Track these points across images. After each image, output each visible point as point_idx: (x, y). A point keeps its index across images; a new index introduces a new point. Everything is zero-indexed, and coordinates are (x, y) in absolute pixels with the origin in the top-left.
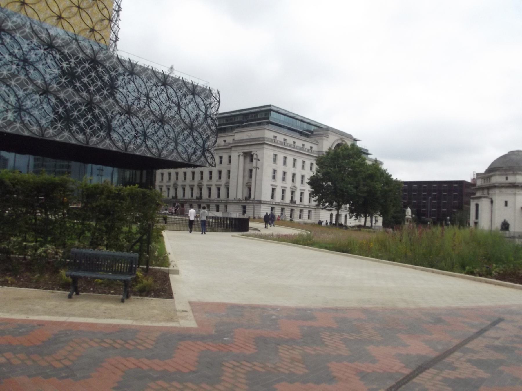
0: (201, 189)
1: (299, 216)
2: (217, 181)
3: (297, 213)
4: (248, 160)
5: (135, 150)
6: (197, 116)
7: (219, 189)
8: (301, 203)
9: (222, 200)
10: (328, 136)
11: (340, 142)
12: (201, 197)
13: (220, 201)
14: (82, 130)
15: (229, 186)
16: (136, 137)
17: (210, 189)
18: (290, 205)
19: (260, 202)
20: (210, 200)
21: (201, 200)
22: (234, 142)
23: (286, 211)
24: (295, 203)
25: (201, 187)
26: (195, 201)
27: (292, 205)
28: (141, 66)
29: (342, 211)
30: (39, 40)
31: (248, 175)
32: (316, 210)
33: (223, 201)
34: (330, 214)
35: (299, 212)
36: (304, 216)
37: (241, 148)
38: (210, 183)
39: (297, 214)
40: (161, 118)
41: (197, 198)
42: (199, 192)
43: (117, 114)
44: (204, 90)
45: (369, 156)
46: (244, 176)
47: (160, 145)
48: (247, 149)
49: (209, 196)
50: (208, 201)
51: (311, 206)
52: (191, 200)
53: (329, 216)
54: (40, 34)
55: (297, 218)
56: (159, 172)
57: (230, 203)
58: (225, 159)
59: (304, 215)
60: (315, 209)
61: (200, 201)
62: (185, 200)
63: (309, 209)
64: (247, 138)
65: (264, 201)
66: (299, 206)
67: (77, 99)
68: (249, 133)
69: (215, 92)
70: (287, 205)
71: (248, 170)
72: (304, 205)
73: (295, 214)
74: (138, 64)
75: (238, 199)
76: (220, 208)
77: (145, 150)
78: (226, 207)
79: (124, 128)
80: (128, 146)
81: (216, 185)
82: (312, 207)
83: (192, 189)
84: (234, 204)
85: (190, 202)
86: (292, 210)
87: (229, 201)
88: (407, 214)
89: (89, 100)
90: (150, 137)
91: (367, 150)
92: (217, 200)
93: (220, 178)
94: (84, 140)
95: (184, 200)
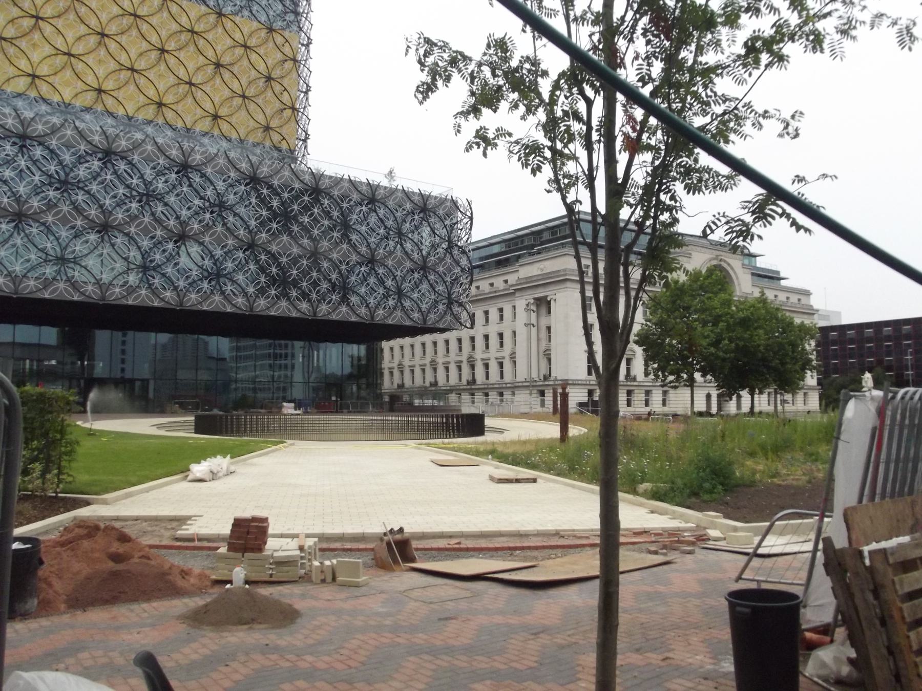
0: (473, 367)
1: (644, 402)
2: (498, 351)
4: (543, 311)
5: (386, 318)
6: (434, 246)
7: (501, 365)
9: (506, 384)
10: (690, 254)
11: (715, 262)
13: (504, 386)
14: (305, 296)
16: (386, 297)
17: (487, 366)
18: (625, 383)
26: (465, 387)
27: (629, 383)
28: (331, 177)
30: (168, 160)
33: (508, 385)
34: (705, 395)
35: (644, 395)
37: (529, 292)
39: (640, 399)
40: (422, 264)
43: (355, 265)
44: (442, 201)
45: (783, 283)
46: (538, 340)
47: (425, 306)
48: (540, 293)
49: (487, 378)
50: (486, 386)
53: (705, 399)
54: (168, 151)
56: (385, 345)
58: (507, 313)
61: (473, 387)
64: (540, 273)
66: (642, 384)
67: (296, 250)
68: (541, 265)
69: (463, 202)
74: (325, 173)
77: (401, 317)
79: (368, 284)
80: (375, 312)
81: (497, 358)
83: (460, 368)
85: (457, 390)
87: (517, 385)
88: (864, 384)
89: (313, 249)
90: (408, 294)
91: (778, 272)
94: (309, 311)
95: (448, 388)
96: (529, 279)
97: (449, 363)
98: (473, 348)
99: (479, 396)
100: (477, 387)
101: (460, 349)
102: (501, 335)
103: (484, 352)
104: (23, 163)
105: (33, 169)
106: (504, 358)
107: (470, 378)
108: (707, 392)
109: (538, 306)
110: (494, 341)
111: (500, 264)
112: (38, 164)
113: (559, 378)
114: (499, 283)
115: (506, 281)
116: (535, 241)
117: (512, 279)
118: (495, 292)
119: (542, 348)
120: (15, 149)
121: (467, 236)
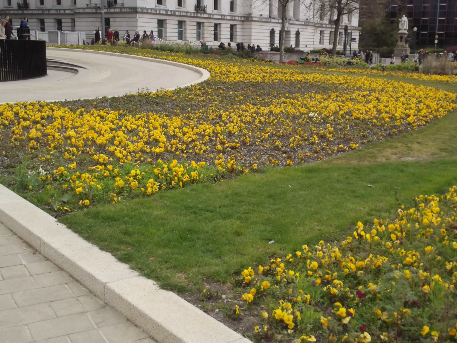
1: (213, 36)
3: (209, 31)
8: (215, 12)
9: (65, 10)
13: (62, 12)
19: (134, 11)
21: (26, 10)
23: (187, 27)
24: (204, 10)
26: (16, 12)
27: (199, 15)
29: (290, 24)
32: (245, 23)
33: (67, 12)
34: (269, 31)
35: (213, 28)
36: (222, 36)
39: (209, 32)
50: (41, 12)
51: (235, 16)
53: (269, 35)
55: (209, 40)
57: (79, 13)
59: (222, 33)
60: (243, 21)
61: (25, 12)
63: (232, 23)
65: (142, 9)
66: (212, 16)
70: (188, 14)
72: (222, 15)
73: (205, 32)
75: (93, 6)
76: (63, 24)
78: (73, 21)
82: (237, 18)
84: (87, 16)
86: (199, 25)
87: (78, 11)
92: (56, 10)
108: (271, 28)
113: (126, 6)
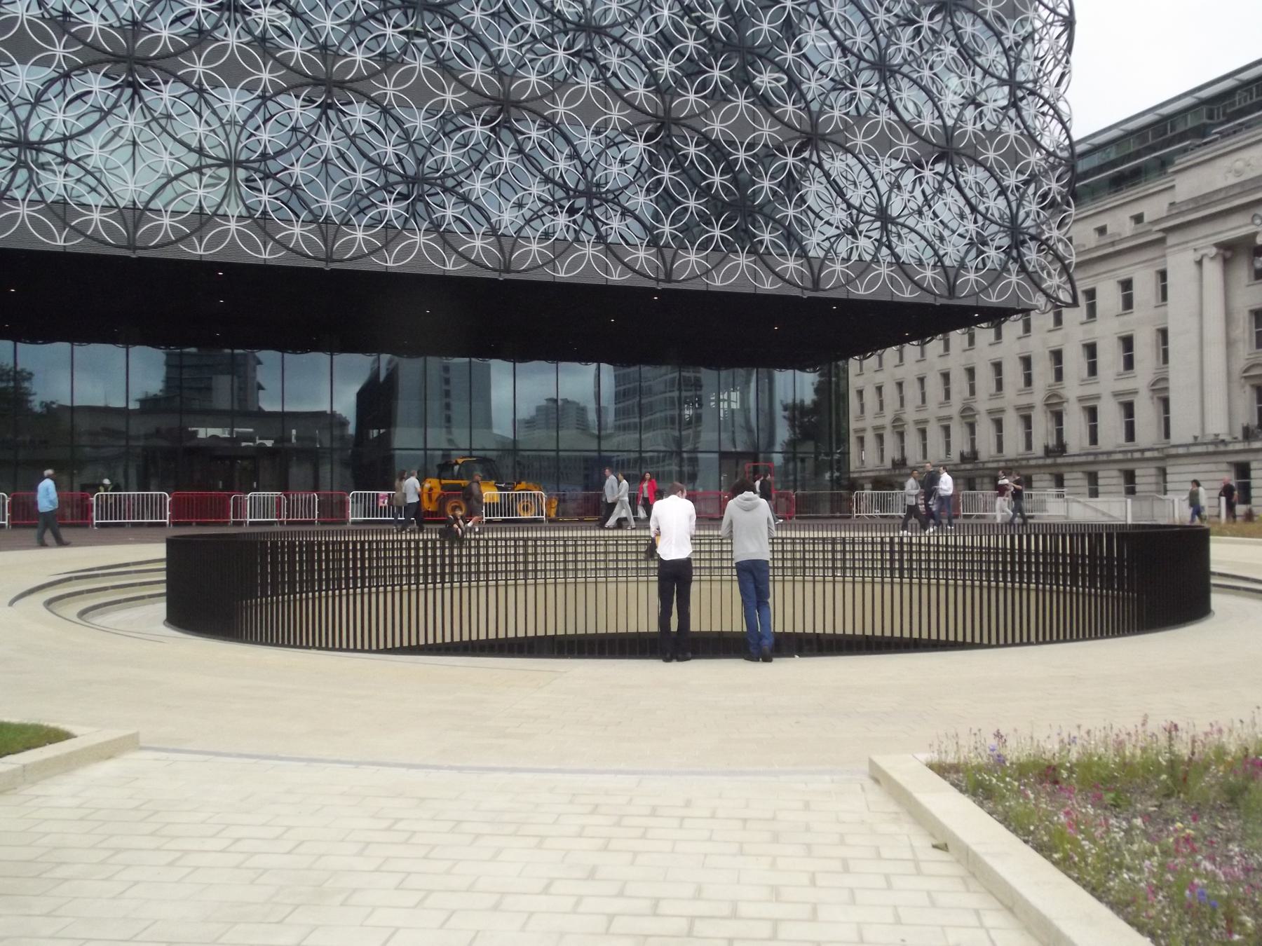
0: (1058, 417)
7: (1129, 409)
9: (1143, 451)
12: (1061, 448)
13: (1137, 455)
15: (1166, 389)
20: (1096, 454)
21: (1060, 456)
22: (1174, 211)
25: (1058, 408)
26: (1041, 462)
31: (1247, 336)
33: (1148, 454)
38: (1090, 390)
41: (1048, 452)
42: (1052, 426)
46: (1230, 344)
49: (1094, 439)
50: (1091, 458)
52: (1024, 463)
58: (1144, 289)
61: (1060, 460)
62: (1006, 461)
64: (1232, 180)
71: (1246, 314)
75: (1210, 438)
76: (1137, 480)
78: (1163, 472)
81: (1116, 395)
83: (1027, 421)
84: (1197, 460)
87: (1173, 451)
93: (1129, 363)
95: (1002, 464)
96: (1199, 202)
97: (1002, 411)
98: (1059, 375)
99: (1076, 480)
100: (1070, 460)
101: (1028, 381)
102: (1128, 343)
103: (1083, 383)
104: (329, 143)
105: (352, 156)
106: (1135, 392)
107: (1052, 442)
109: (1226, 263)
110: (1110, 356)
111: (1119, 183)
112: (358, 141)
114: (1120, 223)
115: (1138, 219)
116: (1210, 117)
117: (1154, 208)
118: (1113, 244)
119: (1240, 363)
120: (313, 113)
121: (1058, 71)
